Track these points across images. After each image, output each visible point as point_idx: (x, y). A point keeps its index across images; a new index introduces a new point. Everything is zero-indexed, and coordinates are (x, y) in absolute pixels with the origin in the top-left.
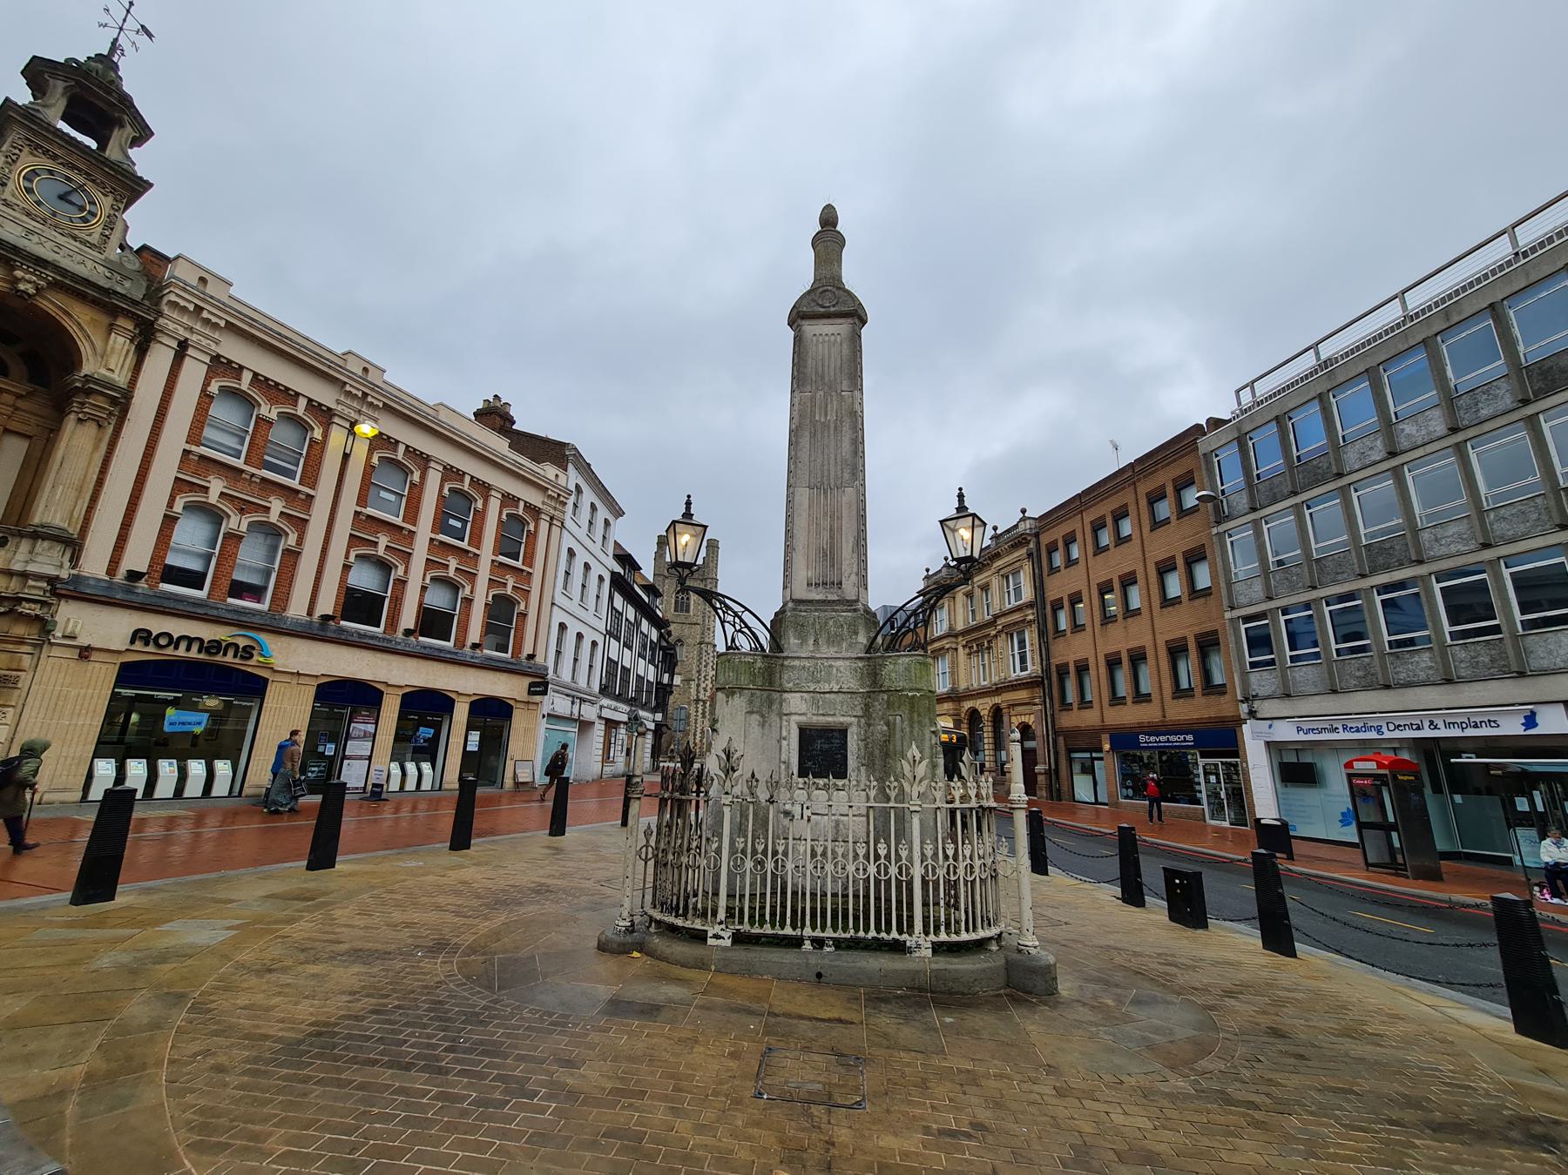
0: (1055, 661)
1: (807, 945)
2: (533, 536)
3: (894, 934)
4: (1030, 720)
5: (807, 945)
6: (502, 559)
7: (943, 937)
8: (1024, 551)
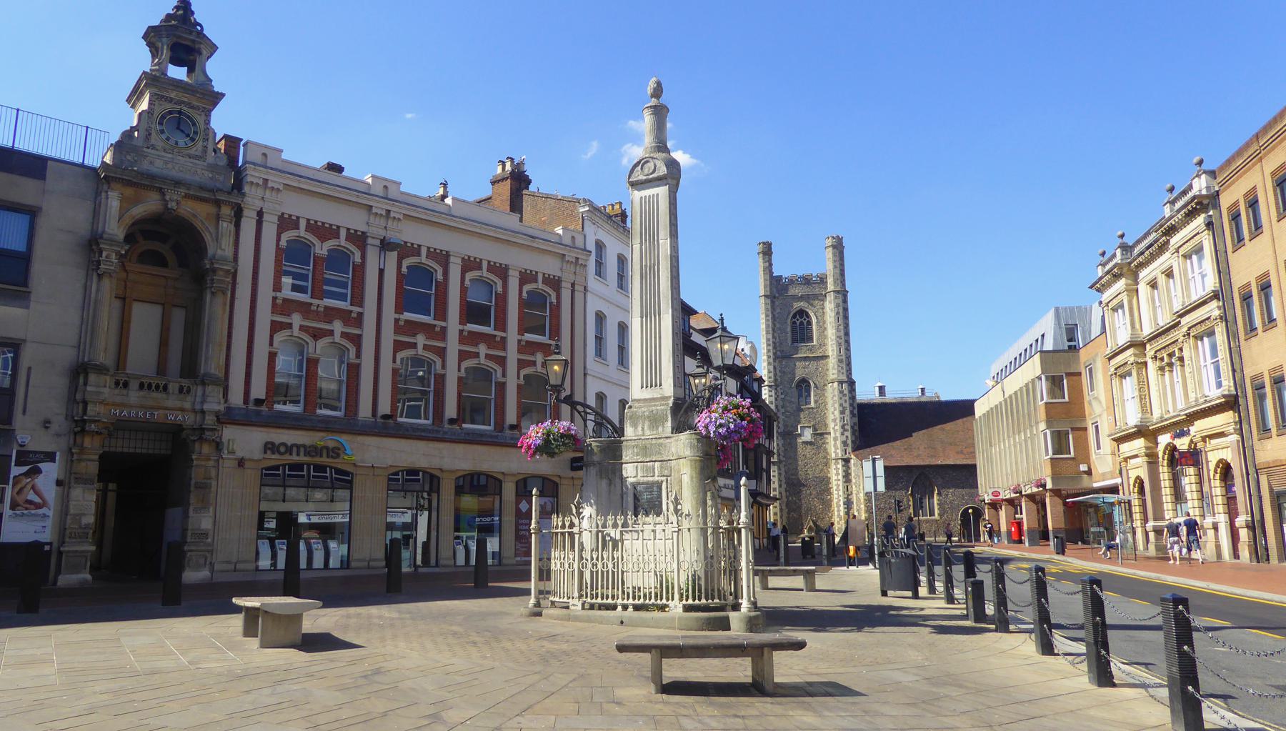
0: (1249, 372)
1: (620, 608)
2: (556, 309)
3: (664, 601)
4: (1229, 456)
5: (620, 608)
6: (529, 337)
7: (690, 601)
8: (1200, 220)
